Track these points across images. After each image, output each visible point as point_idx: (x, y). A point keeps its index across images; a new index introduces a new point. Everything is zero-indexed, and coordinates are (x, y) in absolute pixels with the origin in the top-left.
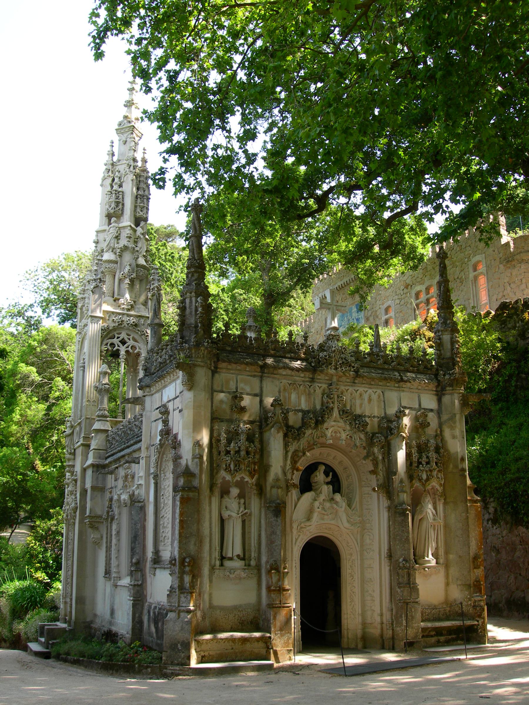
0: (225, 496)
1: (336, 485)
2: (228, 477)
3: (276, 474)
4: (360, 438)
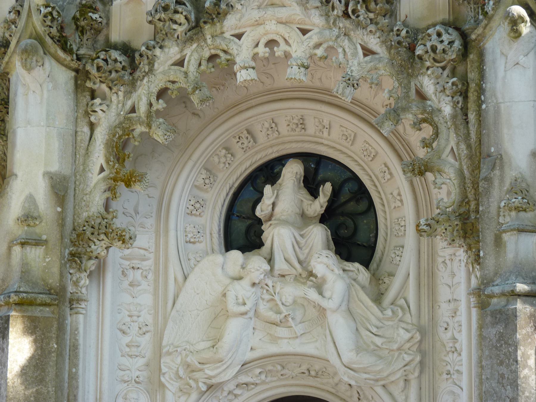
3: (31, 199)
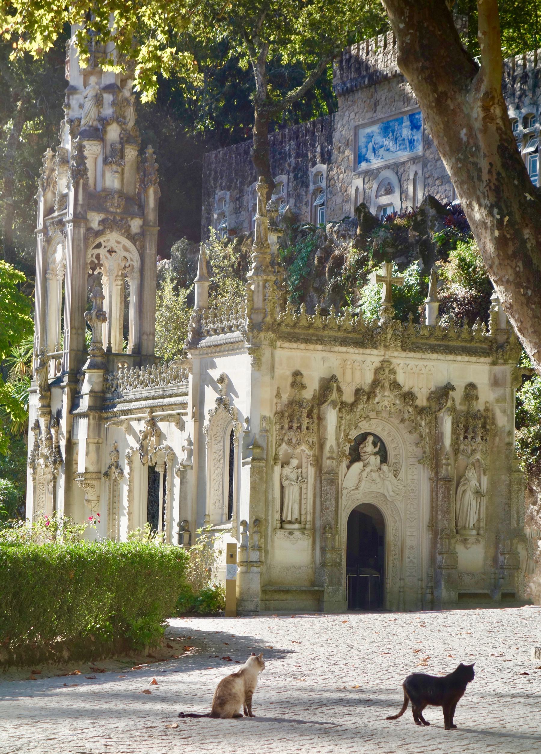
0: (285, 466)
1: (383, 455)
2: (290, 450)
4: (409, 412)
